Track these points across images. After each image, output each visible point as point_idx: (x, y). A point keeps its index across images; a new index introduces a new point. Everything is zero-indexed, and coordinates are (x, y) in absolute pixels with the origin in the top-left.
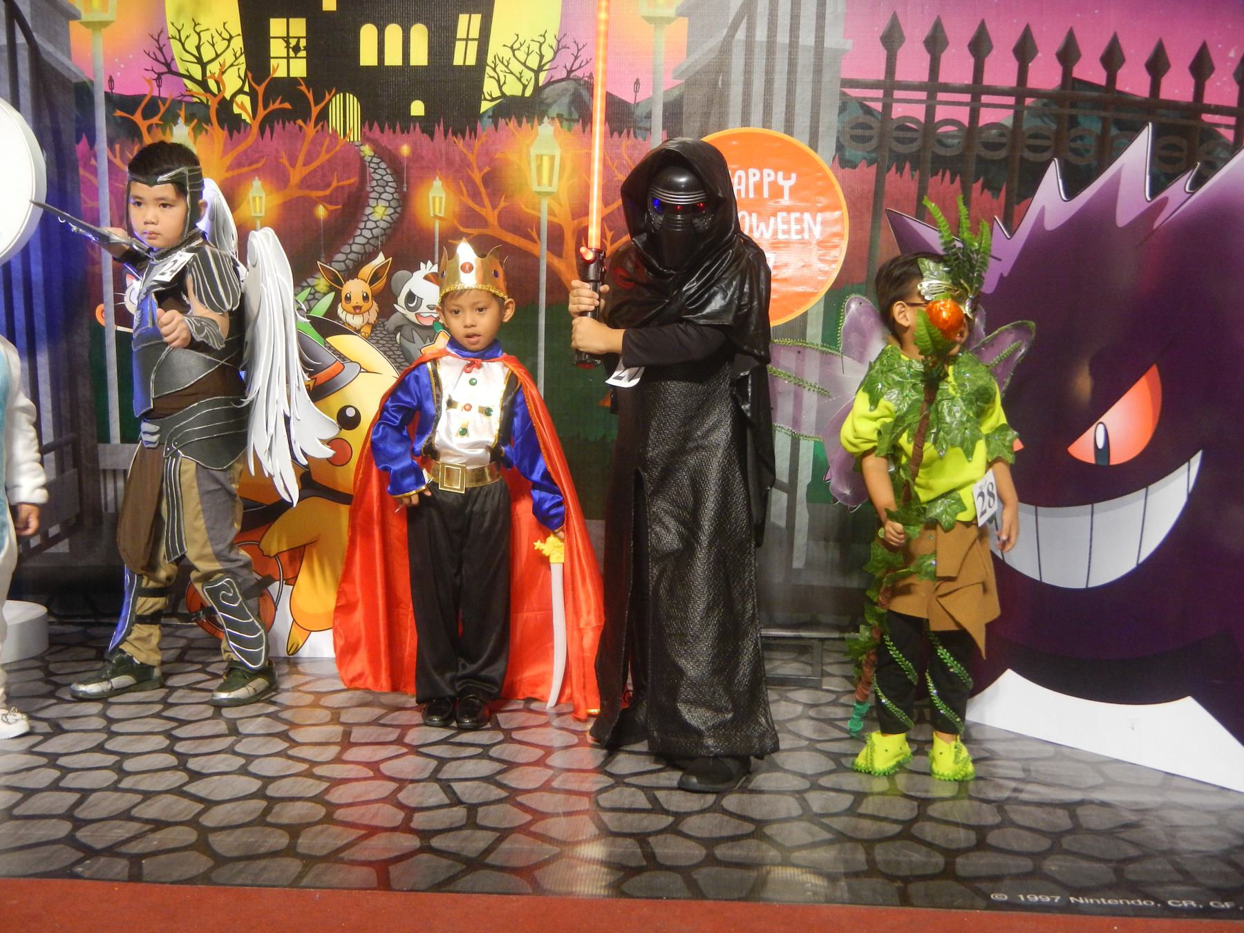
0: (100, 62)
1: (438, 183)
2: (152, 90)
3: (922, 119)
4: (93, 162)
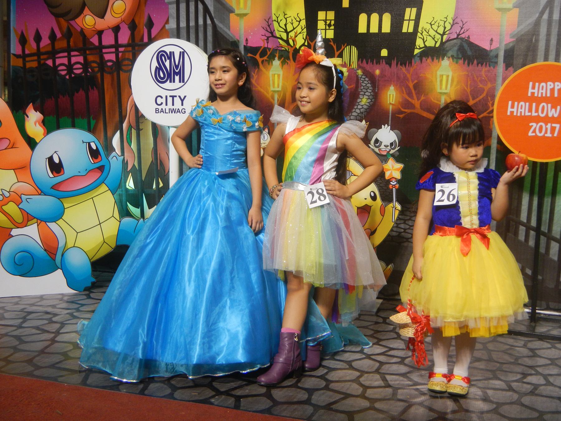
0: (242, 32)
1: (392, 88)
2: (265, 44)
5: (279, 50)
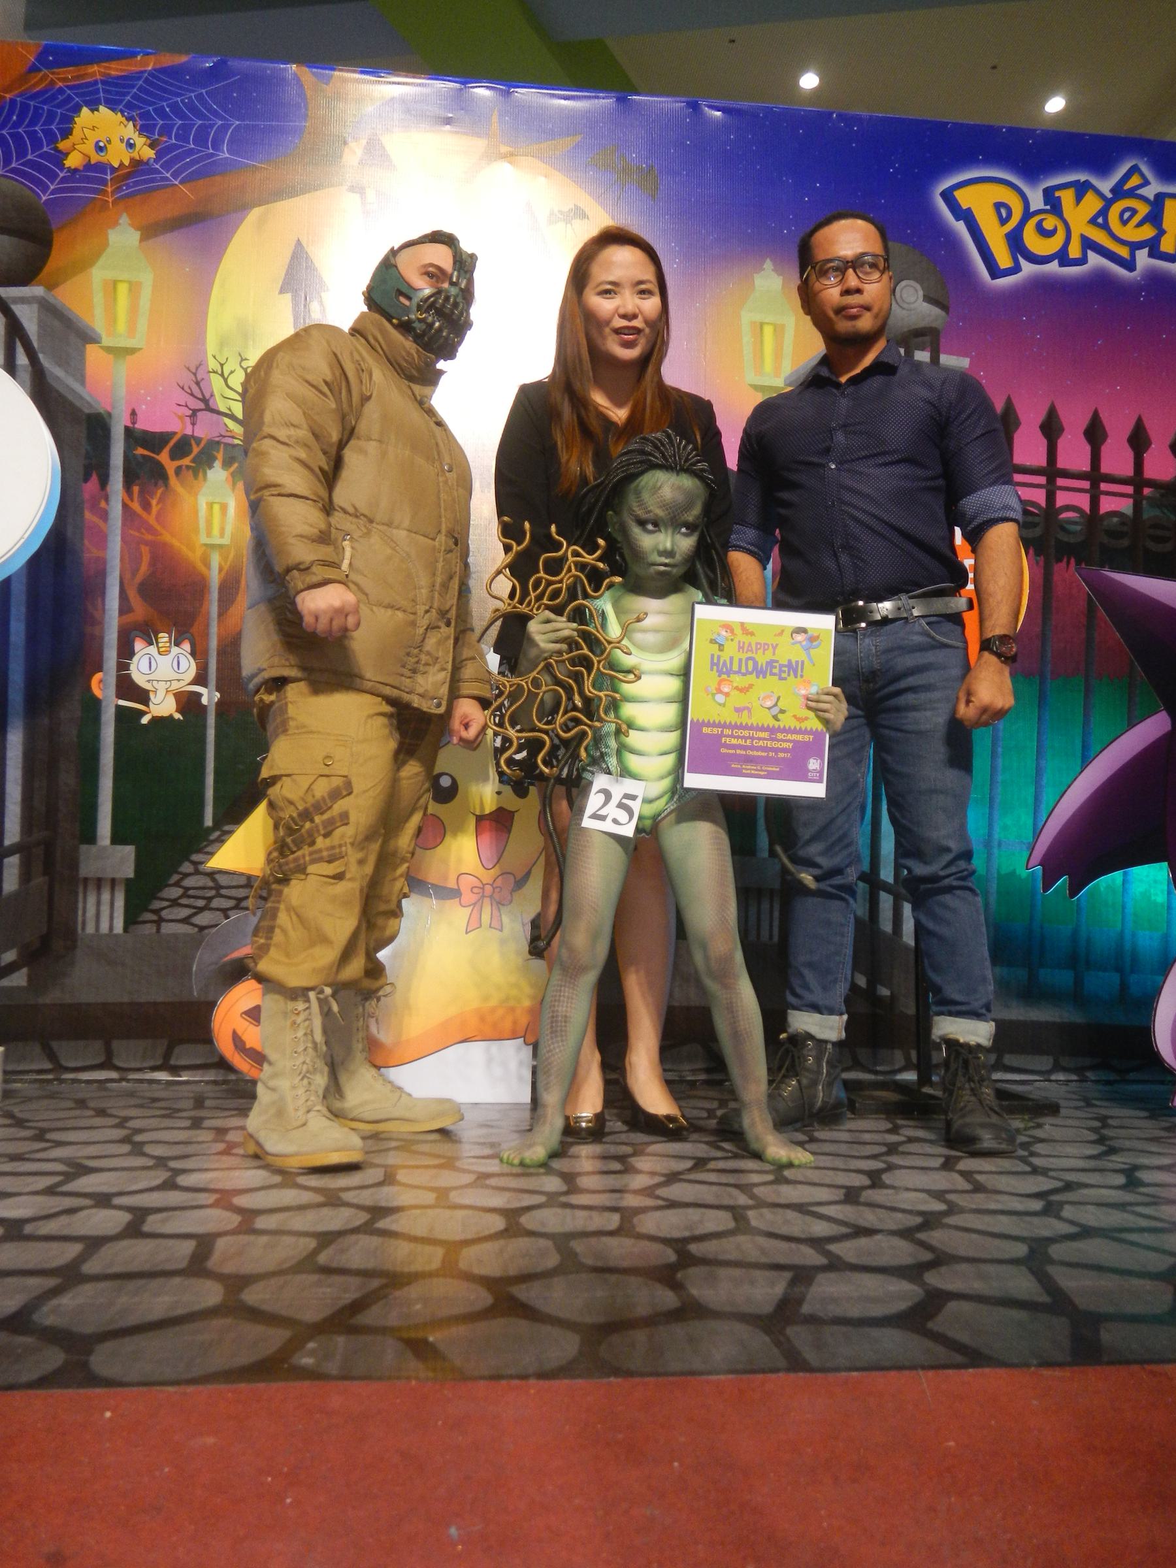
0: (122, 392)
2: (185, 428)
3: (1044, 505)
4: (103, 504)
5: (226, 445)
